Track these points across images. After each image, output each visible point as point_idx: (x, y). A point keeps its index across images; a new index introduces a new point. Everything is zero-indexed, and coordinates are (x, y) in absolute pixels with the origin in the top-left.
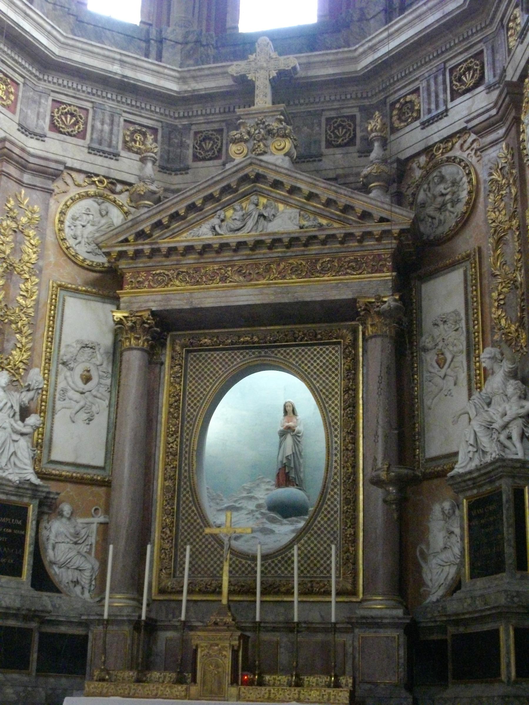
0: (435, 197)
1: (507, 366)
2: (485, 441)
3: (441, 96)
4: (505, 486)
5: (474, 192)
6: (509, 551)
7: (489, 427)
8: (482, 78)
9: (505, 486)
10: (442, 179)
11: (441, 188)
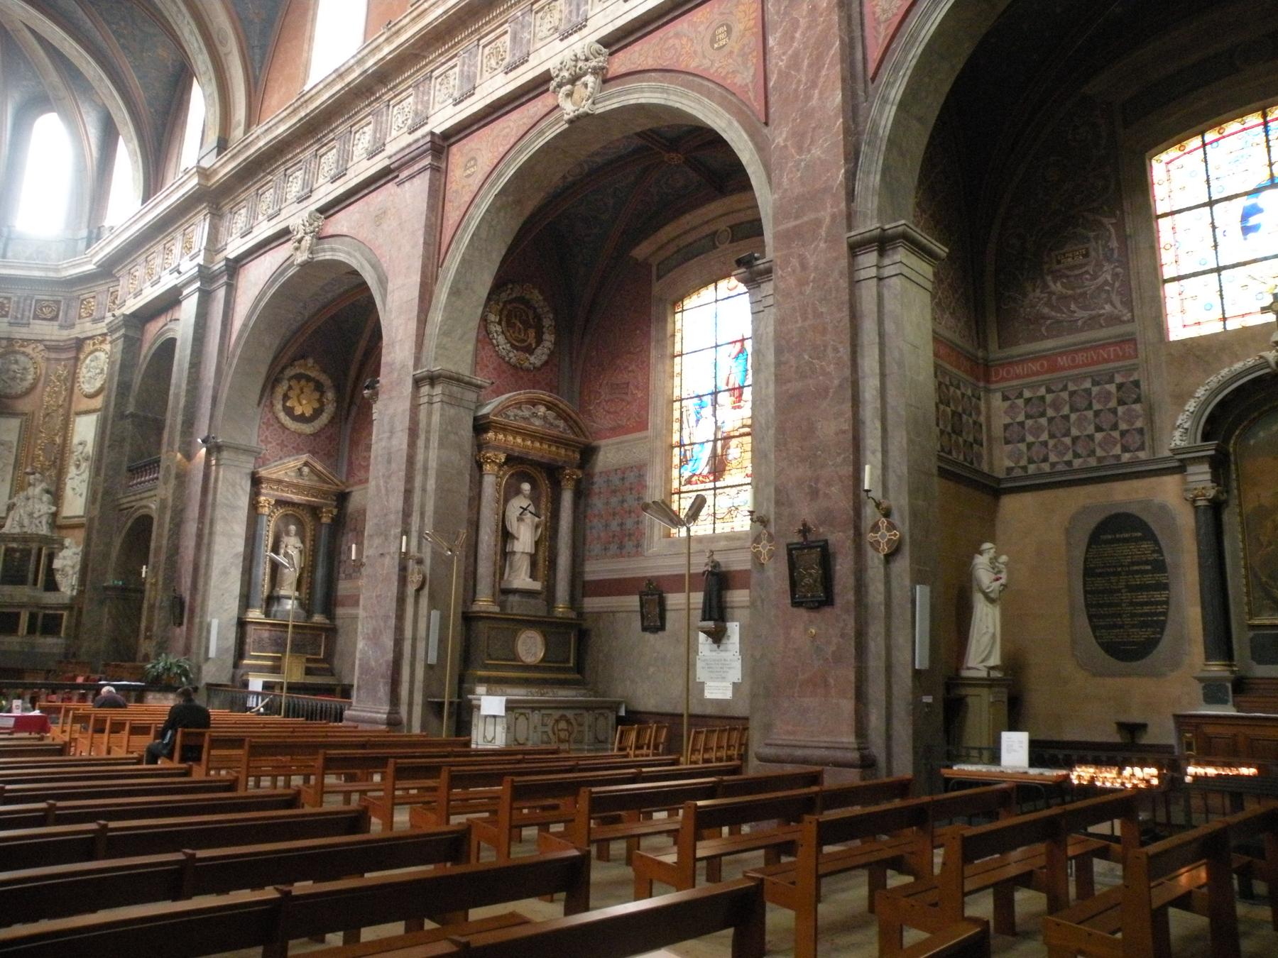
0: (8, 370)
1: (44, 485)
2: (26, 522)
3: (27, 313)
4: (34, 546)
5: (36, 380)
6: (31, 576)
7: (31, 515)
8: (57, 316)
9: (34, 546)
10: (16, 362)
11: (15, 367)
